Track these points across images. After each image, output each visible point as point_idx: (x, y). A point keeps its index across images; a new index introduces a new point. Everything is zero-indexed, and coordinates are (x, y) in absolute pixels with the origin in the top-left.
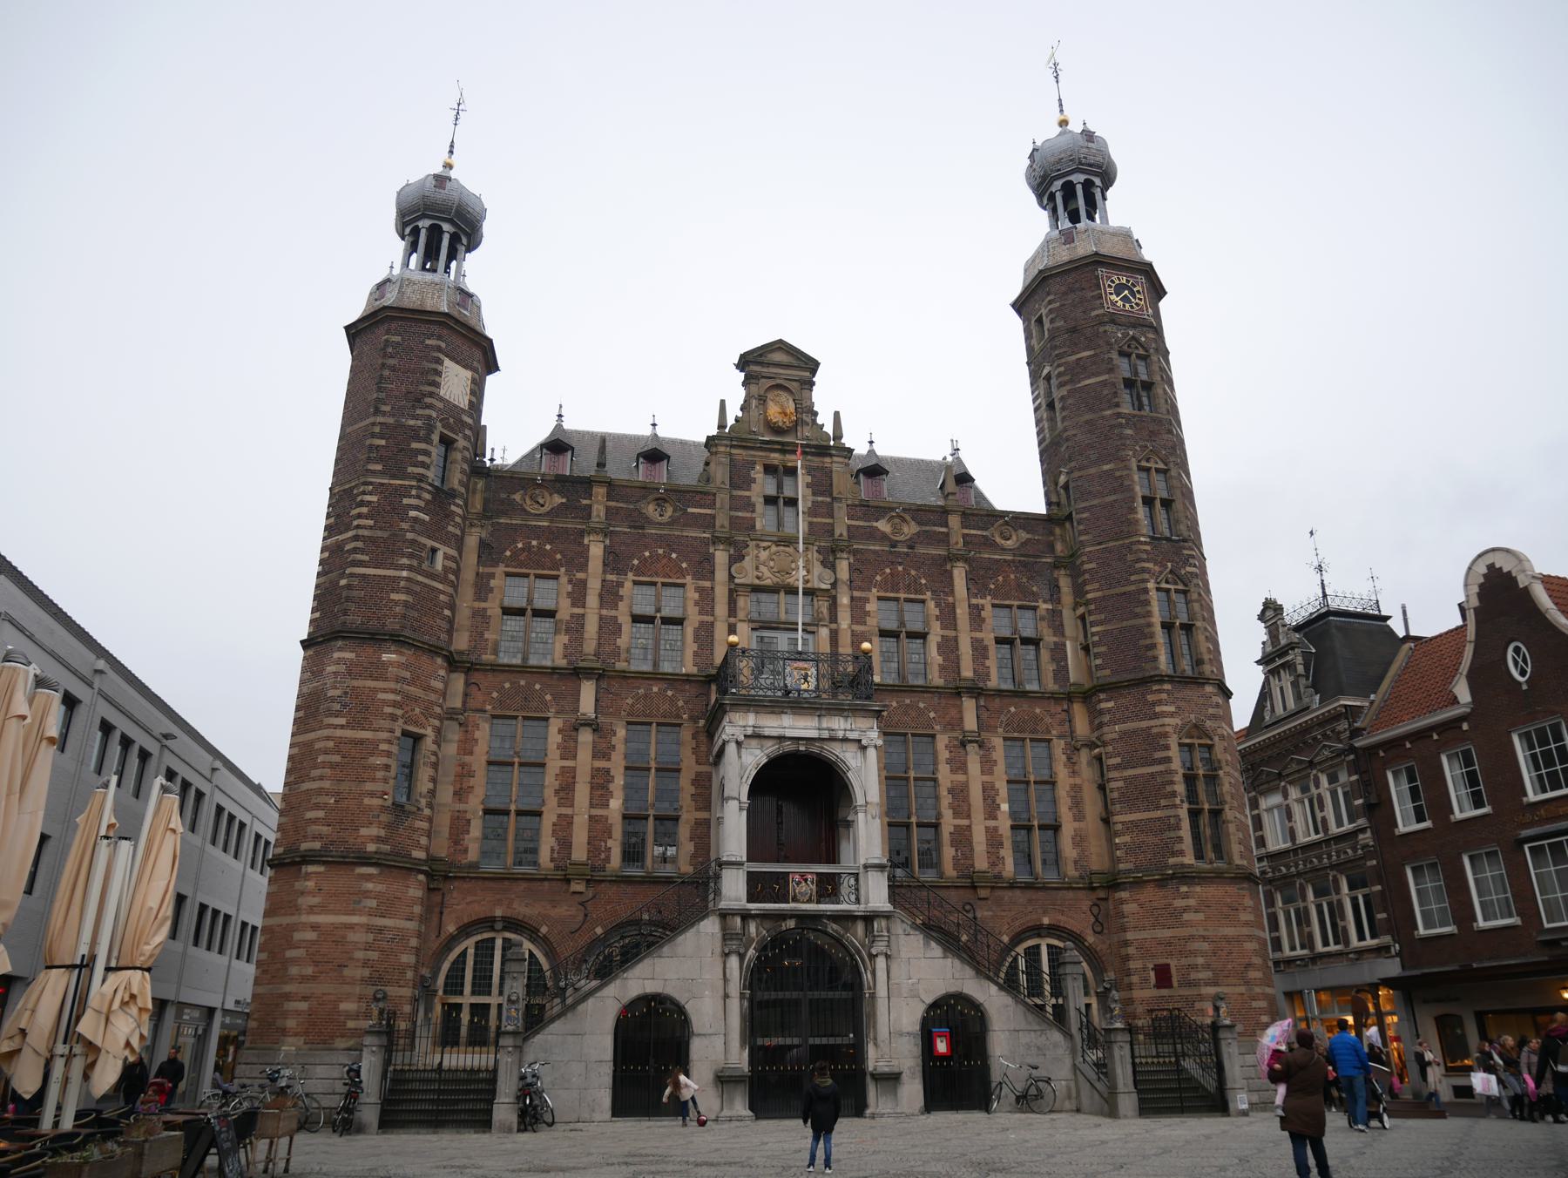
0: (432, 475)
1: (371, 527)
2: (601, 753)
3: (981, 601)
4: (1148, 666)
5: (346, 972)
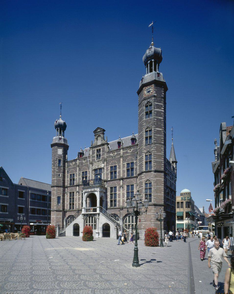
0: (58, 165)
5: (54, 222)
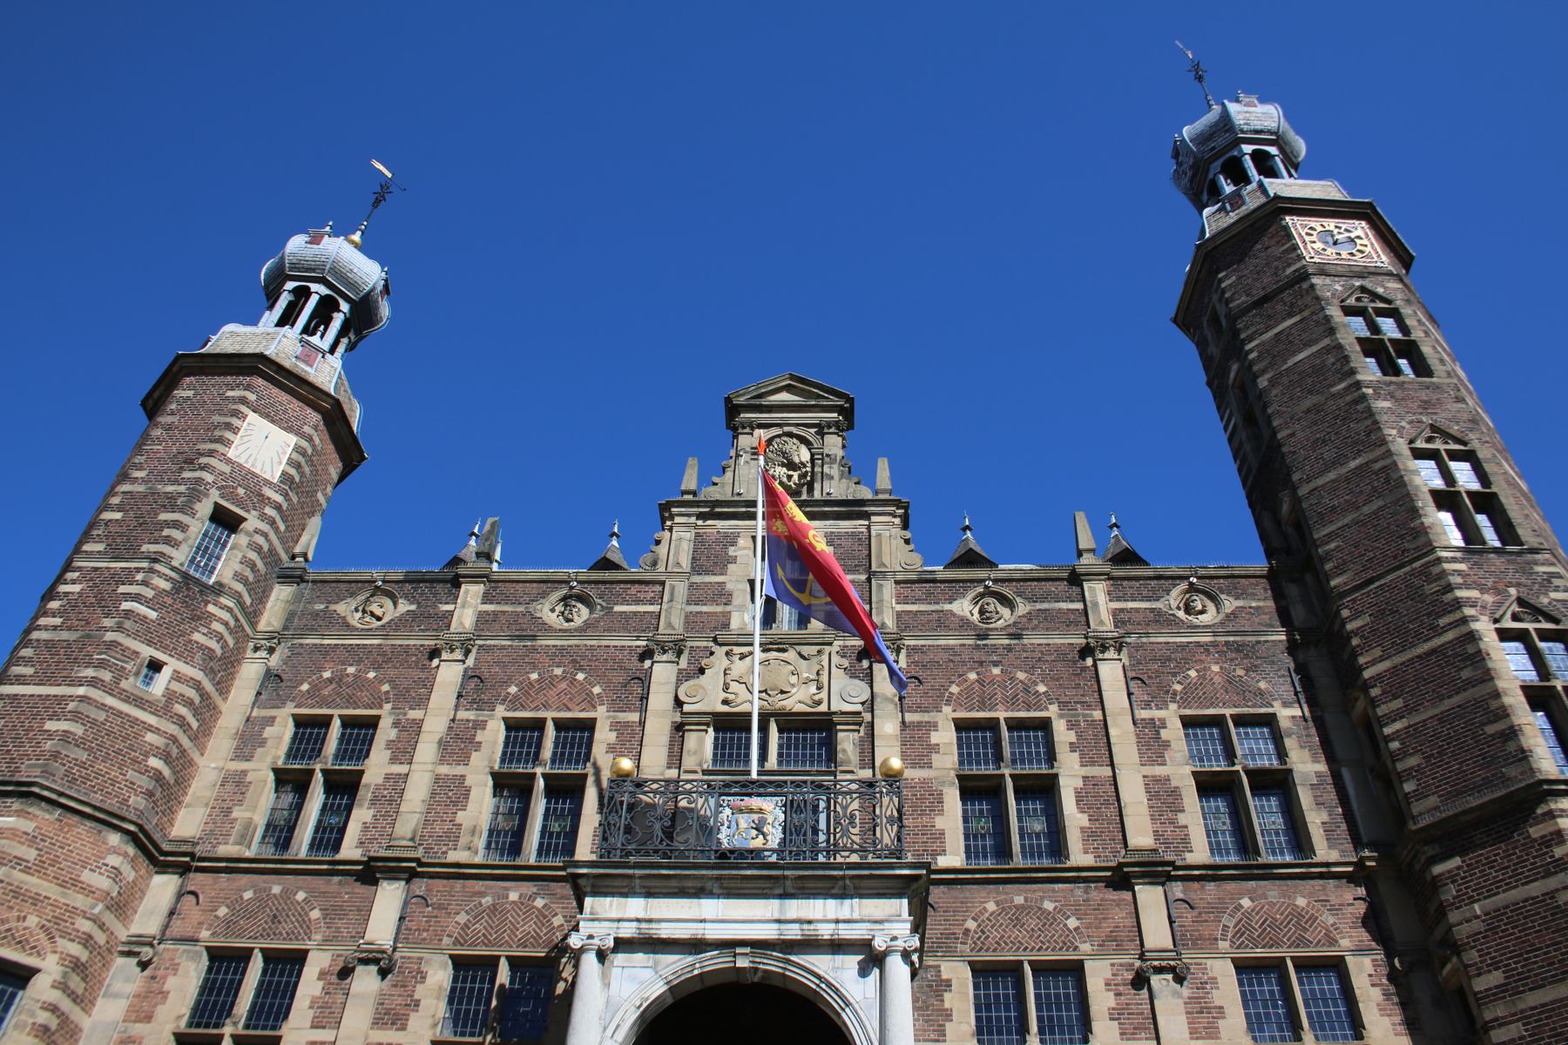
0: (180, 556)
1: (55, 628)
3: (1157, 714)
4: (1511, 771)
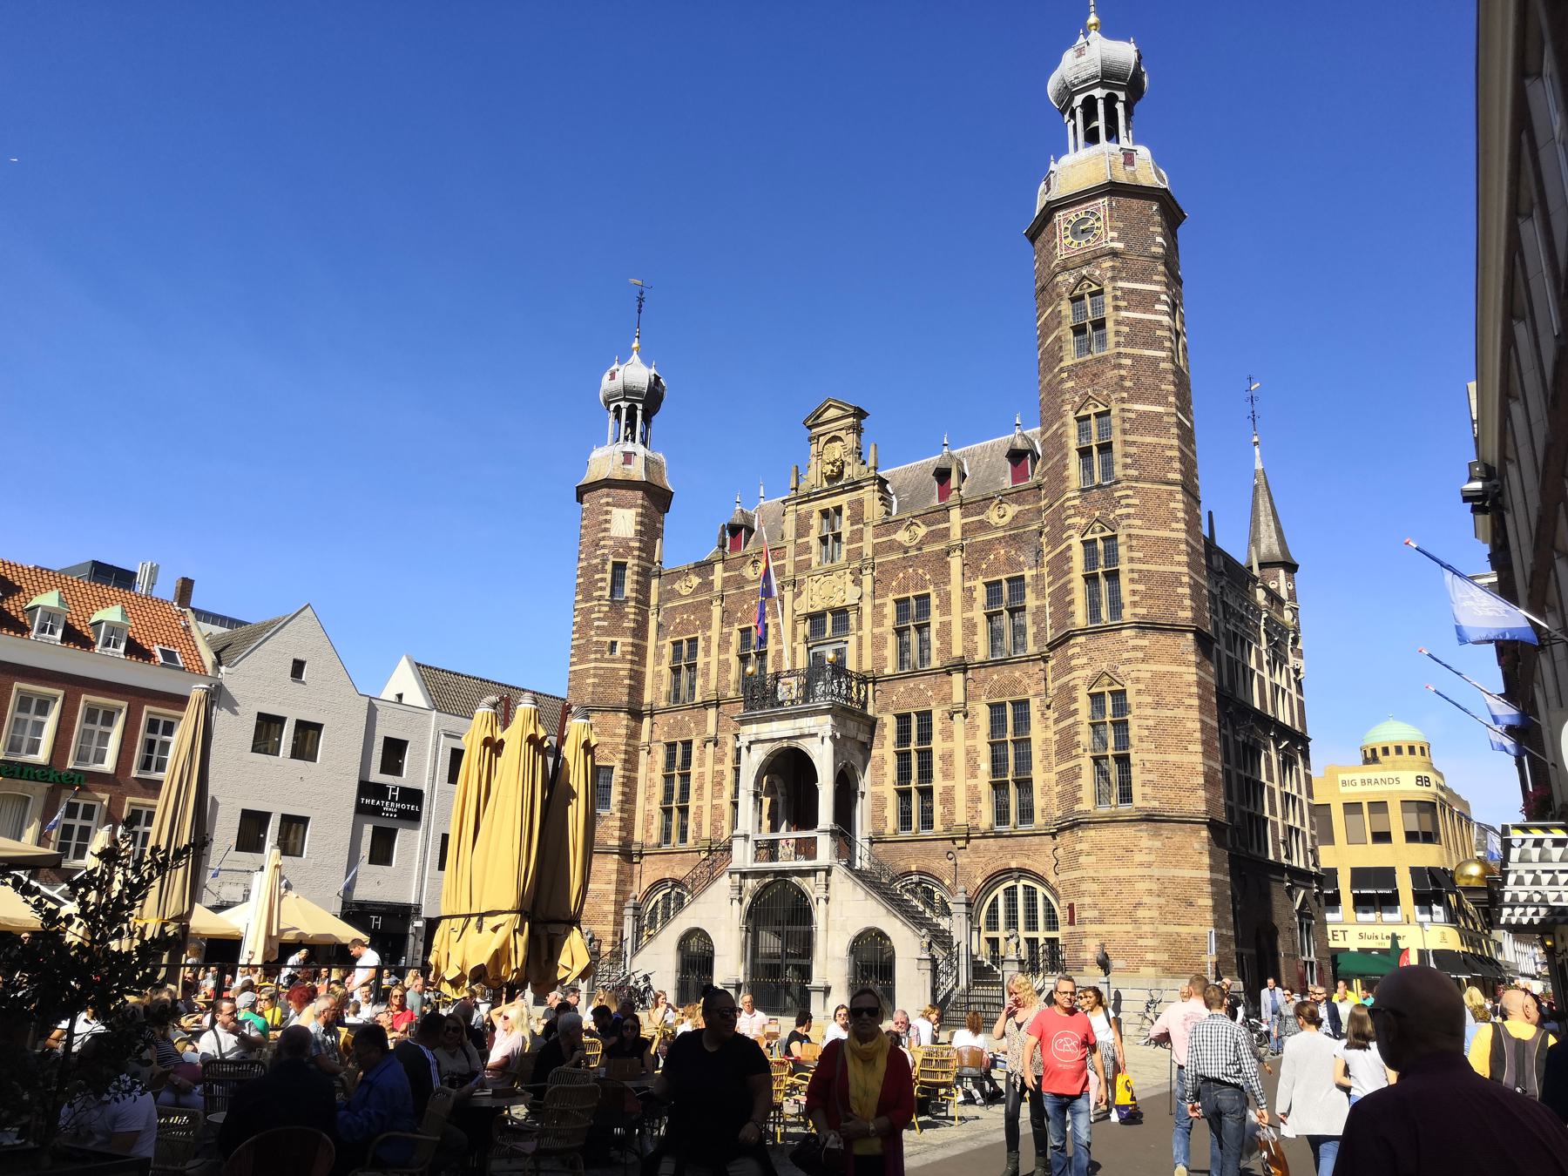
0: (607, 593)
2: (719, 760)
